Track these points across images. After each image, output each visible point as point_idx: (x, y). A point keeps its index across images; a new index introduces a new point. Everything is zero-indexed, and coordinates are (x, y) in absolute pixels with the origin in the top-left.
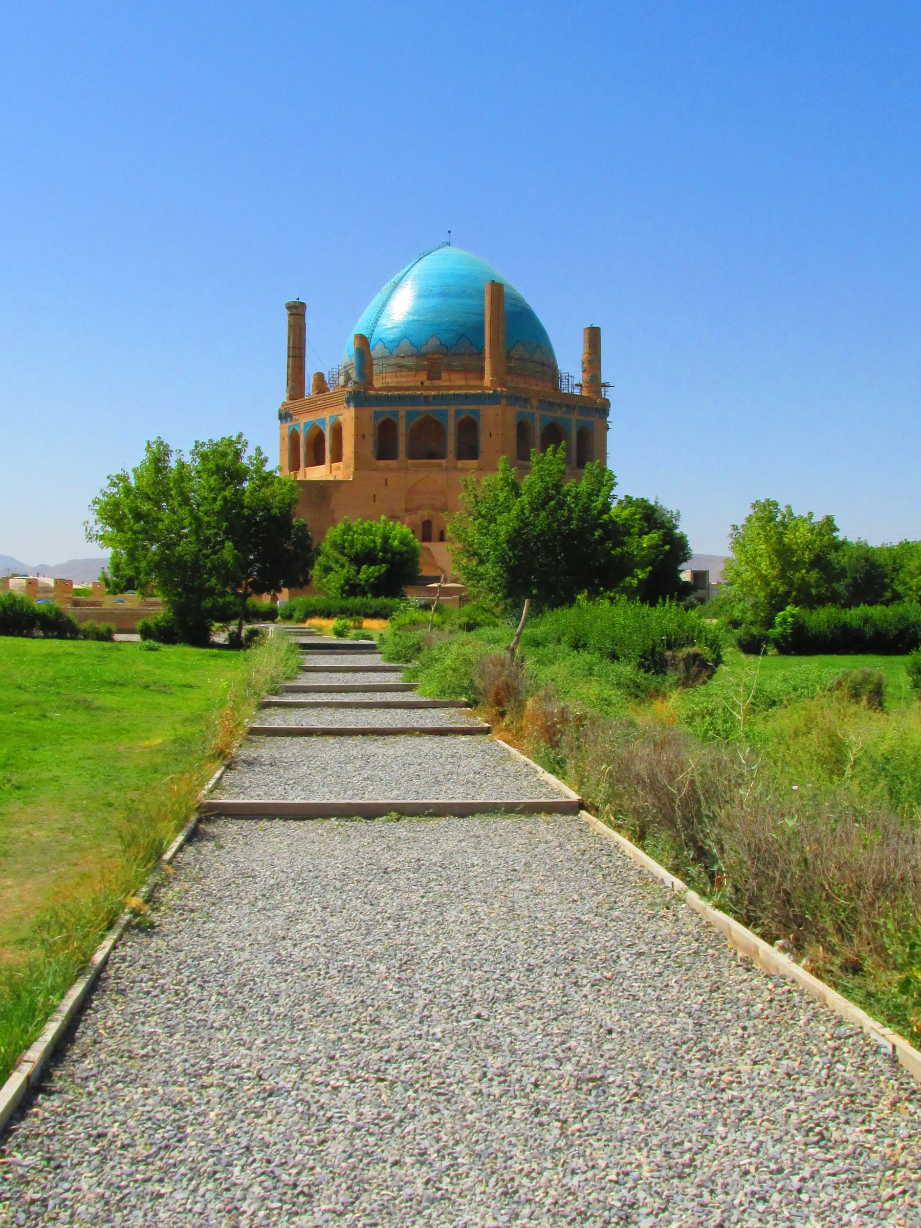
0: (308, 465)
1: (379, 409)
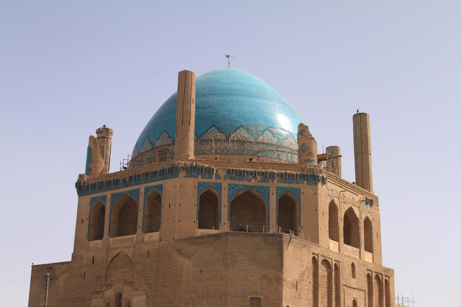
1: (94, 196)
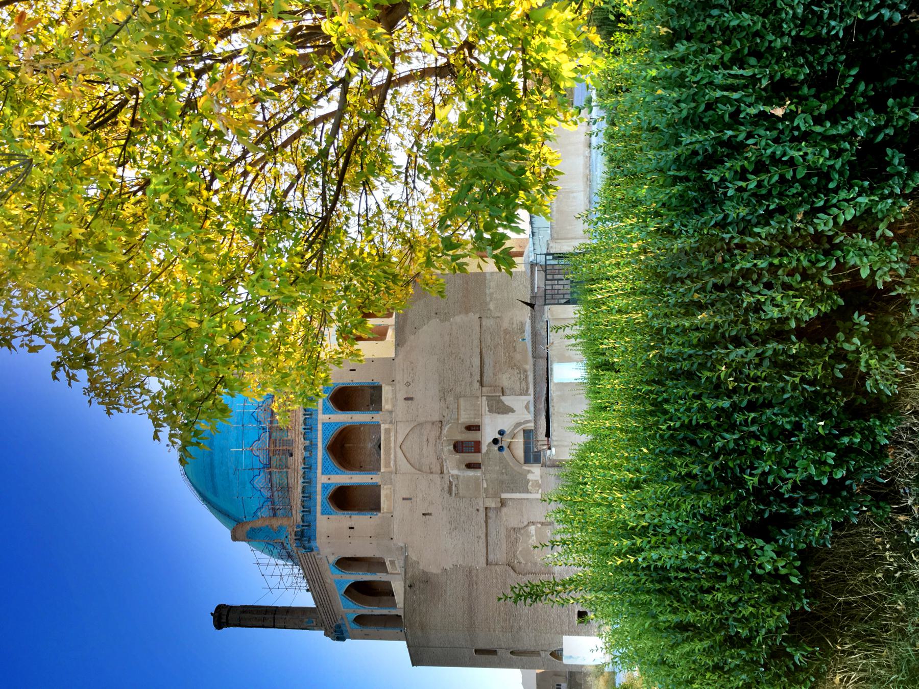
0: (394, 605)
1: (319, 508)
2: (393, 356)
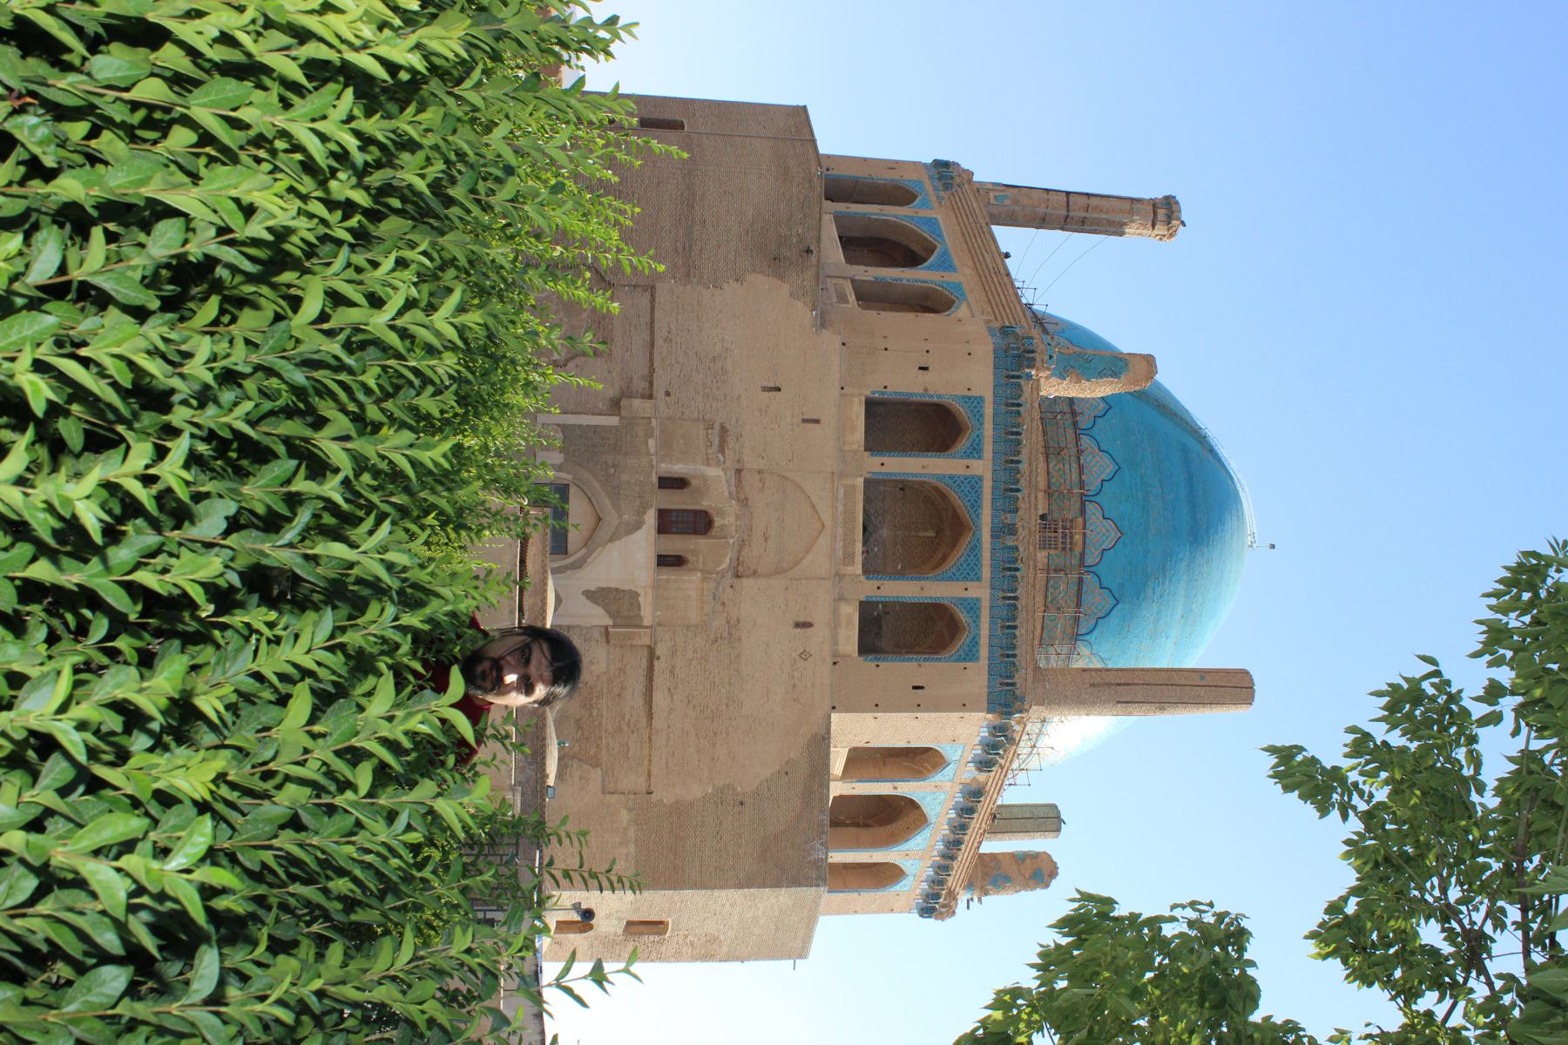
0: (839, 219)
1: (988, 410)
2: (834, 717)
